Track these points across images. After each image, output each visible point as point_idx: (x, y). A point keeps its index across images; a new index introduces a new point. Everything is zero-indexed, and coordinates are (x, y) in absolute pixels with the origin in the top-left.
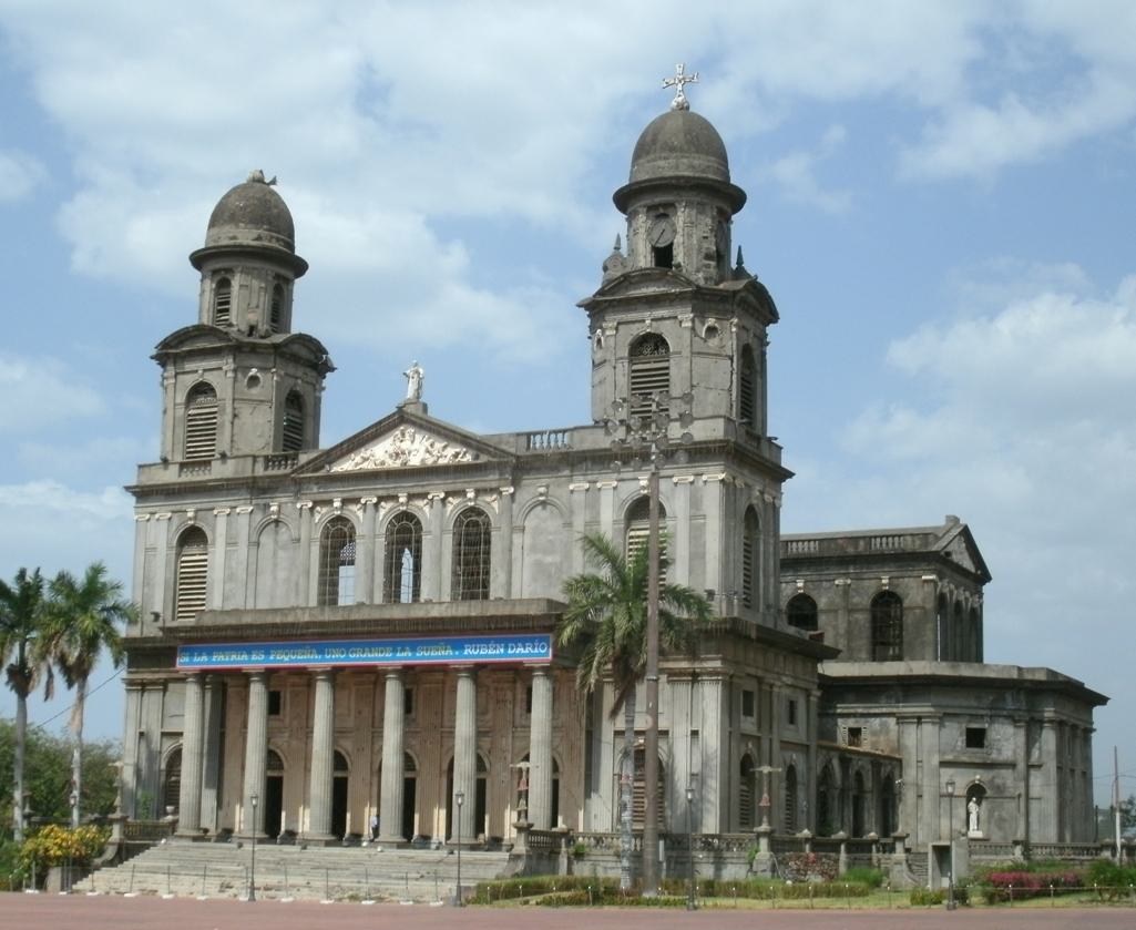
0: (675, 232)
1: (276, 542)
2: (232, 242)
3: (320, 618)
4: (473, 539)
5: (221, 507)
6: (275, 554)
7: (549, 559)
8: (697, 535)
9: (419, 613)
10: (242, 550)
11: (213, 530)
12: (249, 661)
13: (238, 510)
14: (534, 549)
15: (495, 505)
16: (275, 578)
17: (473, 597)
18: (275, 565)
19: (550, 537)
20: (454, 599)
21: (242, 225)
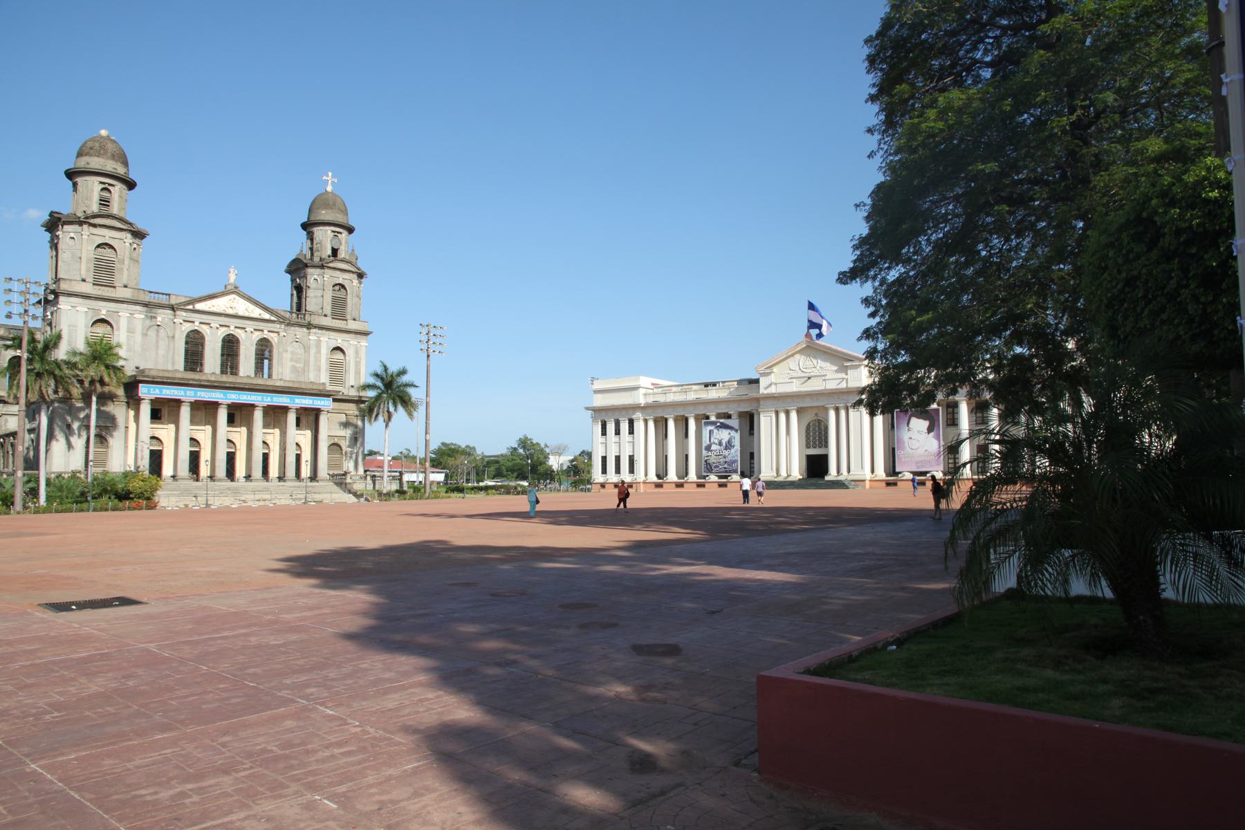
0: (341, 244)
1: (157, 336)
2: (113, 171)
3: (221, 380)
4: (264, 351)
5: (124, 312)
6: (157, 342)
7: (298, 365)
8: (358, 364)
9: (270, 383)
10: (138, 337)
11: (118, 323)
12: (185, 396)
13: (135, 316)
14: (292, 360)
15: (276, 339)
16: (157, 354)
17: (193, 370)
18: (157, 348)
19: (299, 356)
20: (186, 370)
21: (119, 164)
